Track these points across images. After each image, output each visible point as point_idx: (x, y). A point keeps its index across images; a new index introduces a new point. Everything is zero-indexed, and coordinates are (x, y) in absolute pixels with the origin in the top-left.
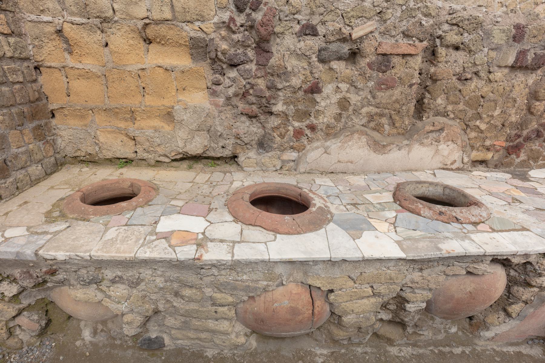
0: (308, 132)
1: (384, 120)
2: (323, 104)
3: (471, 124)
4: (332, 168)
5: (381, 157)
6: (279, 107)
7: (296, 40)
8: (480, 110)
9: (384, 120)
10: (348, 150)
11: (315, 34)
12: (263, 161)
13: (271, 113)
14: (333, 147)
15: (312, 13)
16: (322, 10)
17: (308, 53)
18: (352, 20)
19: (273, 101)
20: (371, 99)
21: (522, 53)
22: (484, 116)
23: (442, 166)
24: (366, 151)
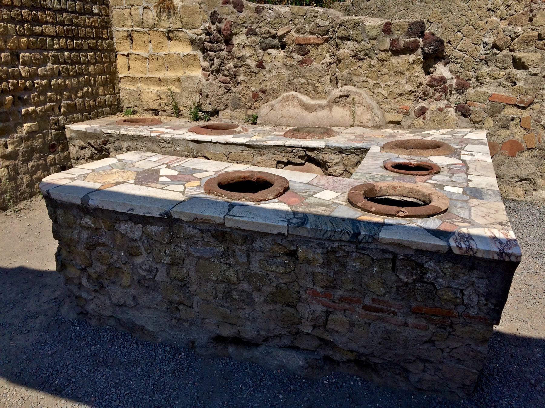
3: (376, 91)
4: (278, 121)
6: (241, 78)
7: (246, 37)
8: (379, 81)
9: (310, 87)
10: (287, 108)
11: (256, 34)
12: (235, 115)
13: (238, 83)
15: (253, 23)
16: (257, 20)
17: (253, 45)
18: (276, 25)
19: (237, 74)
20: (299, 73)
21: (394, 42)
22: (383, 85)
24: (300, 110)
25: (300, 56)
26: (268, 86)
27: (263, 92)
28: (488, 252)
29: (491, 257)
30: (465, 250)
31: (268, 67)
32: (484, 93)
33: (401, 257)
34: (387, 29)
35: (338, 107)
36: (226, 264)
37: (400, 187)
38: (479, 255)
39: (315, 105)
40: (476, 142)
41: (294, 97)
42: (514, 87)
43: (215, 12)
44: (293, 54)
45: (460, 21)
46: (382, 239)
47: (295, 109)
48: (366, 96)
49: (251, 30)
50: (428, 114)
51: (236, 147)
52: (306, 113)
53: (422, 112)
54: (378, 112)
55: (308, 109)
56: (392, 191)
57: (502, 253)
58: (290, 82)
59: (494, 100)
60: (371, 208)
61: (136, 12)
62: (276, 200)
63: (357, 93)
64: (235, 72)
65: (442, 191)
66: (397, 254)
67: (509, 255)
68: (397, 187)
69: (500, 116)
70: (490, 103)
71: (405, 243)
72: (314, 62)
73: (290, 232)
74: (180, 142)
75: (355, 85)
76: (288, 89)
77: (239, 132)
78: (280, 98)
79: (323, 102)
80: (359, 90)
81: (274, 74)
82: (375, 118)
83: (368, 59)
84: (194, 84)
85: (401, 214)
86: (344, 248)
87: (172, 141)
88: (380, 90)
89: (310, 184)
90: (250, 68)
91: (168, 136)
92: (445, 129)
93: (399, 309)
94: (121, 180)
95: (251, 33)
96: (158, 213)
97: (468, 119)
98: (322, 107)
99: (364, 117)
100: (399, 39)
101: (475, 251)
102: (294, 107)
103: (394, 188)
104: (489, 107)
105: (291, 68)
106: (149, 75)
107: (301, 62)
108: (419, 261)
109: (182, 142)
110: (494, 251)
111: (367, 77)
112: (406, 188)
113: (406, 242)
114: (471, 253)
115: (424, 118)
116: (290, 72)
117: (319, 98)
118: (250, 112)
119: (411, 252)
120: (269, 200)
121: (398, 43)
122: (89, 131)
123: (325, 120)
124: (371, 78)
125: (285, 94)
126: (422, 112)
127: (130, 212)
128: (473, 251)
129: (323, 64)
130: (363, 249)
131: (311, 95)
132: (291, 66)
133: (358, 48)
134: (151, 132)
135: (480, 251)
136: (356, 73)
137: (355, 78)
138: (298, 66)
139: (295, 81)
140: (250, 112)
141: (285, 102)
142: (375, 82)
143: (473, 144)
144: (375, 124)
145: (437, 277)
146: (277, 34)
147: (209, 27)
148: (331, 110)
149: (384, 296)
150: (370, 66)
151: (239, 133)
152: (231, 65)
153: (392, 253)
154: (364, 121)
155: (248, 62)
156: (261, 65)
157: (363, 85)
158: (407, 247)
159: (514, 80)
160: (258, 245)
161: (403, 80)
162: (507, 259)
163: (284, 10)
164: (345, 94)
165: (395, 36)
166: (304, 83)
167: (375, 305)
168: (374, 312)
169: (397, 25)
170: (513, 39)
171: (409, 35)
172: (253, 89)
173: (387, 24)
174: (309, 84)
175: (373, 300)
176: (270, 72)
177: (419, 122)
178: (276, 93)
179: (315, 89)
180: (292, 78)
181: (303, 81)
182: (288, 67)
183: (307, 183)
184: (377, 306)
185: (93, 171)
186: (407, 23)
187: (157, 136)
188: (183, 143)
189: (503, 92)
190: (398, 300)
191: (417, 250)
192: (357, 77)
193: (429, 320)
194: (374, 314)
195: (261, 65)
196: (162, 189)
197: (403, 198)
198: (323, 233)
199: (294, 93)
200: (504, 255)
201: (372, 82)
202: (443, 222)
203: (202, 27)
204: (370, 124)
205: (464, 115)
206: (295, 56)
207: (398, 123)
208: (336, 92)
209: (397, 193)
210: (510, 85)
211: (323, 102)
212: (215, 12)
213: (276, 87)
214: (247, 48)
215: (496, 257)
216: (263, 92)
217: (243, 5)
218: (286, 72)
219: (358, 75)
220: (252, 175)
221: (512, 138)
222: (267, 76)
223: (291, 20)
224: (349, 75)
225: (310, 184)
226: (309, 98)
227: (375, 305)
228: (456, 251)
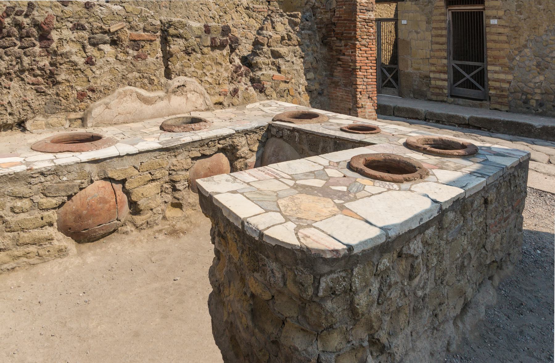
0: (90, 94)
1: (146, 81)
2: (98, 72)
3: (203, 79)
6: (61, 77)
8: (205, 71)
14: (112, 103)
20: (133, 68)
22: (208, 74)
23: (195, 109)
26: (99, 84)
39: (155, 97)
44: (128, 49)
47: (134, 104)
50: (240, 93)
51: (148, 154)
53: (236, 91)
55: (148, 102)
58: (124, 77)
75: (186, 75)
76: (121, 85)
82: (207, 101)
83: (194, 53)
88: (206, 78)
97: (263, 94)
105: (125, 63)
109: (72, 168)
115: (238, 97)
116: (125, 67)
123: (164, 111)
125: (120, 90)
126: (236, 91)
136: (187, 65)
137: (186, 70)
138: (133, 61)
139: (130, 76)
141: (121, 98)
144: (207, 107)
148: (169, 101)
150: (196, 59)
154: (198, 106)
164: (182, 84)
172: (79, 88)
177: (235, 100)
179: (151, 82)
180: (127, 73)
181: (137, 75)
192: (187, 68)
201: (200, 72)
204: (203, 108)
205: (261, 92)
207: (221, 103)
213: (108, 84)
214: (71, 44)
216: (93, 91)
218: (120, 67)
222: (98, 72)
224: (181, 68)
226: (146, 91)
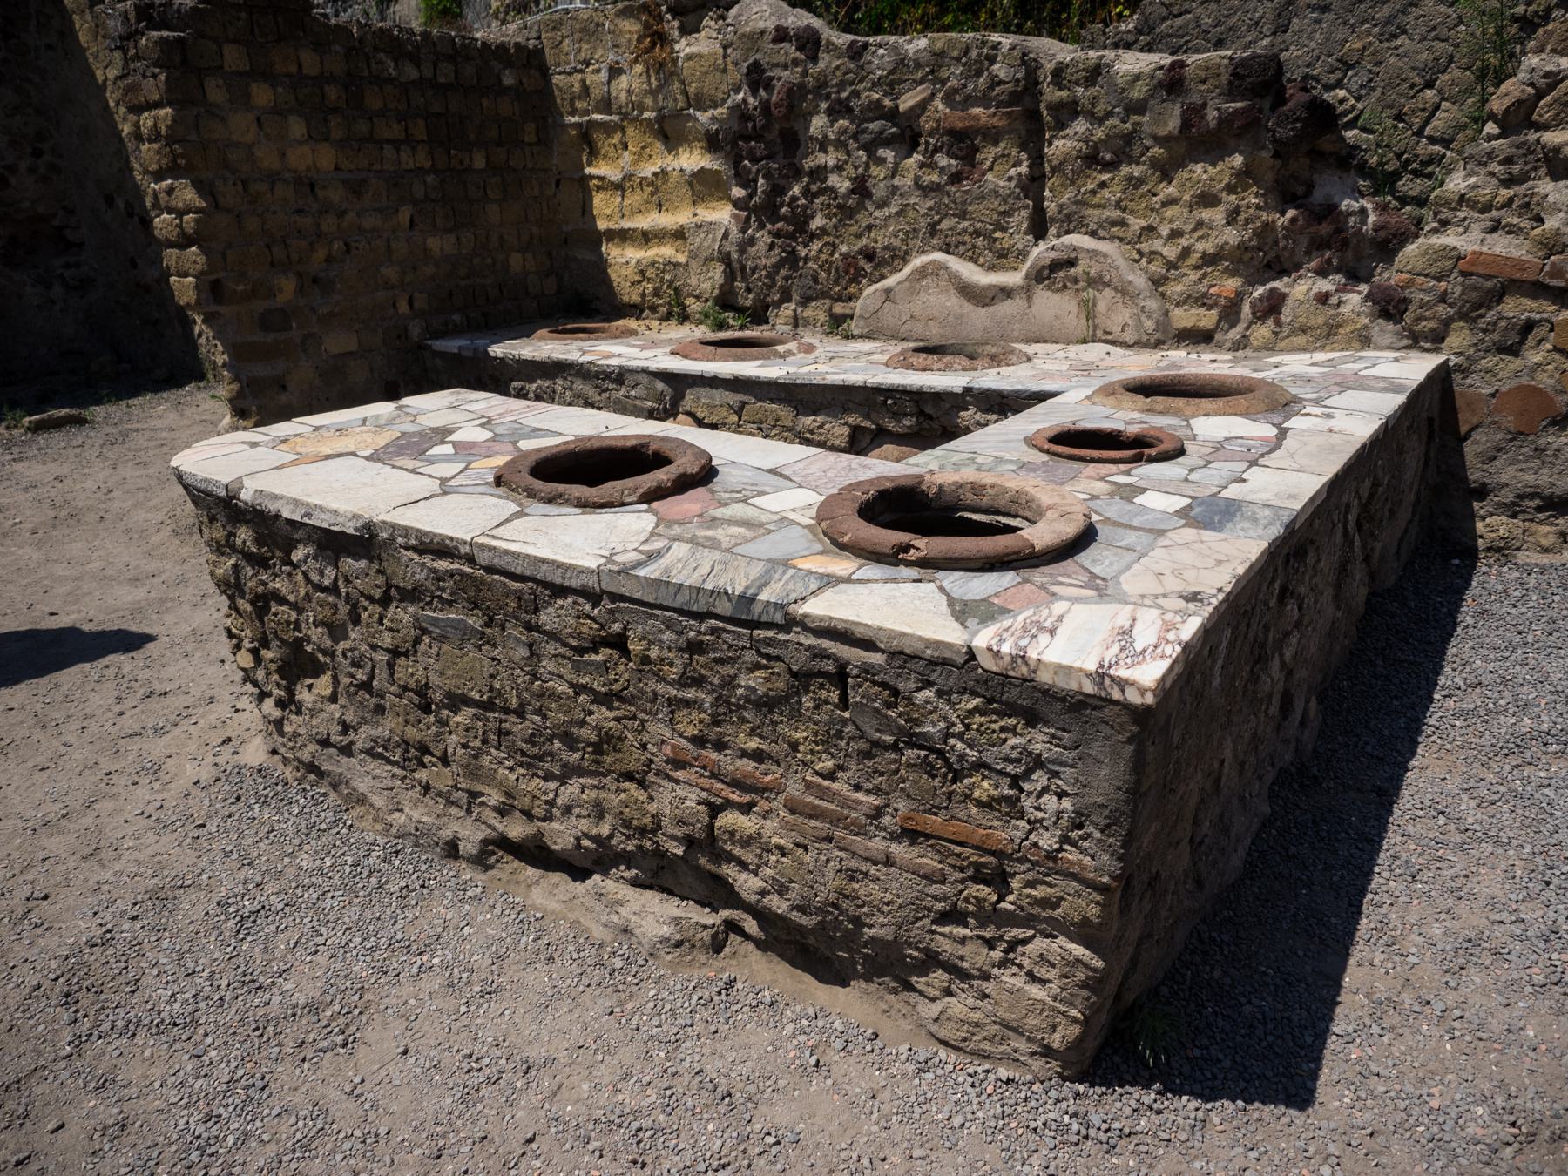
0: (862, 263)
5: (982, 311)
6: (817, 222)
21: (1192, 115)
25: (953, 162)
26: (880, 240)
27: (869, 255)
28: (1068, 670)
29: (1074, 686)
30: (1008, 659)
31: (879, 191)
32: (1444, 248)
33: (855, 672)
34: (1172, 83)
35: (1049, 293)
36: (493, 659)
37: (992, 486)
38: (1044, 677)
39: (991, 287)
40: (1382, 384)
41: (940, 268)
42: (1537, 231)
43: (756, 64)
45: (1431, 57)
46: (805, 616)
48: (1121, 262)
49: (839, 101)
52: (968, 307)
54: (1153, 304)
56: (970, 495)
57: (1102, 676)
58: (933, 230)
59: (1473, 269)
60: (843, 534)
61: (595, 78)
62: (645, 506)
63: (1094, 253)
64: (805, 207)
65: (1128, 507)
66: (848, 663)
67: (1122, 684)
68: (983, 487)
69: (1491, 316)
70: (1461, 279)
71: (860, 632)
72: (989, 176)
73: (604, 586)
74: (636, 376)
75: (1093, 234)
77: (790, 353)
78: (907, 270)
79: (1014, 278)
80: (1104, 246)
81: (894, 209)
82: (1143, 319)
84: (714, 240)
85: (912, 555)
86: (724, 635)
87: (620, 376)
89: (781, 475)
90: (835, 198)
91: (614, 362)
92: (1333, 350)
93: (868, 816)
94: (352, 448)
95: (839, 109)
96: (351, 524)
98: (1006, 292)
99: (1113, 317)
100: (1204, 105)
101: (1032, 664)
102: (941, 292)
103: (978, 489)
104: (1459, 289)
106: (626, 224)
107: (956, 178)
108: (901, 686)
110: (1081, 670)
111: (1124, 210)
112: (1006, 490)
113: (861, 629)
114: (1024, 670)
117: (1002, 268)
118: (839, 308)
119: (877, 659)
120: (623, 504)
121: (1203, 117)
122: (465, 353)
124: (1132, 212)
127: (306, 520)
128: (1027, 664)
129: (1010, 179)
130: (769, 642)
131: (981, 260)
132: (936, 188)
133: (1100, 134)
134: (584, 353)
135: (1046, 664)
136: (1096, 200)
139: (945, 224)
140: (839, 308)
142: (1144, 223)
143: (1363, 388)
144: (1145, 338)
145: (947, 735)
146: (897, 107)
147: (744, 101)
148: (1029, 299)
149: (831, 776)
151: (783, 356)
152: (796, 189)
153: (837, 659)
154: (1116, 329)
155: (833, 180)
156: (861, 189)
157: (1112, 228)
158: (868, 645)
159: (1536, 209)
160: (547, 618)
161: (1217, 215)
162: (1116, 695)
163: (917, 45)
164: (1063, 255)
165: (1195, 99)
166: (965, 231)
167: (810, 799)
168: (811, 817)
169: (1199, 67)
170: (1540, 95)
171: (1231, 93)
172: (844, 248)
173: (1173, 65)
174: (977, 233)
175: (809, 786)
176: (883, 204)
177: (1263, 332)
178: (897, 258)
180: (936, 218)
182: (926, 190)
183: (770, 471)
184: (817, 802)
185: (317, 429)
186: (1226, 61)
187: (590, 363)
188: (644, 379)
189: (1501, 245)
190: (868, 792)
191: (893, 654)
192: (1097, 212)
193: (944, 856)
194: (813, 823)
195: (861, 189)
196: (412, 471)
197: (999, 518)
198: (672, 591)
199: (939, 256)
200: (1107, 681)
202: (1026, 581)
203: (729, 103)
206: (942, 160)
208: (1040, 252)
209: (985, 501)
210: (1526, 224)
211: (1014, 278)
212: (756, 64)
213: (895, 242)
215: (1089, 688)
217: (818, 43)
219: (1099, 206)
220: (642, 445)
221: (1526, 380)
223: (932, 72)
225: (781, 475)
227: (810, 799)
228: (987, 662)
